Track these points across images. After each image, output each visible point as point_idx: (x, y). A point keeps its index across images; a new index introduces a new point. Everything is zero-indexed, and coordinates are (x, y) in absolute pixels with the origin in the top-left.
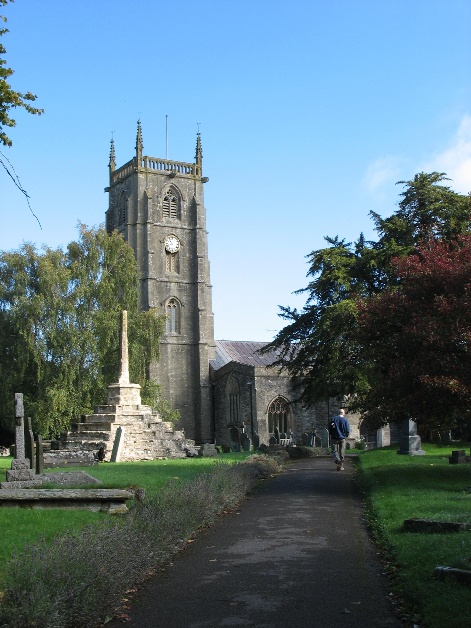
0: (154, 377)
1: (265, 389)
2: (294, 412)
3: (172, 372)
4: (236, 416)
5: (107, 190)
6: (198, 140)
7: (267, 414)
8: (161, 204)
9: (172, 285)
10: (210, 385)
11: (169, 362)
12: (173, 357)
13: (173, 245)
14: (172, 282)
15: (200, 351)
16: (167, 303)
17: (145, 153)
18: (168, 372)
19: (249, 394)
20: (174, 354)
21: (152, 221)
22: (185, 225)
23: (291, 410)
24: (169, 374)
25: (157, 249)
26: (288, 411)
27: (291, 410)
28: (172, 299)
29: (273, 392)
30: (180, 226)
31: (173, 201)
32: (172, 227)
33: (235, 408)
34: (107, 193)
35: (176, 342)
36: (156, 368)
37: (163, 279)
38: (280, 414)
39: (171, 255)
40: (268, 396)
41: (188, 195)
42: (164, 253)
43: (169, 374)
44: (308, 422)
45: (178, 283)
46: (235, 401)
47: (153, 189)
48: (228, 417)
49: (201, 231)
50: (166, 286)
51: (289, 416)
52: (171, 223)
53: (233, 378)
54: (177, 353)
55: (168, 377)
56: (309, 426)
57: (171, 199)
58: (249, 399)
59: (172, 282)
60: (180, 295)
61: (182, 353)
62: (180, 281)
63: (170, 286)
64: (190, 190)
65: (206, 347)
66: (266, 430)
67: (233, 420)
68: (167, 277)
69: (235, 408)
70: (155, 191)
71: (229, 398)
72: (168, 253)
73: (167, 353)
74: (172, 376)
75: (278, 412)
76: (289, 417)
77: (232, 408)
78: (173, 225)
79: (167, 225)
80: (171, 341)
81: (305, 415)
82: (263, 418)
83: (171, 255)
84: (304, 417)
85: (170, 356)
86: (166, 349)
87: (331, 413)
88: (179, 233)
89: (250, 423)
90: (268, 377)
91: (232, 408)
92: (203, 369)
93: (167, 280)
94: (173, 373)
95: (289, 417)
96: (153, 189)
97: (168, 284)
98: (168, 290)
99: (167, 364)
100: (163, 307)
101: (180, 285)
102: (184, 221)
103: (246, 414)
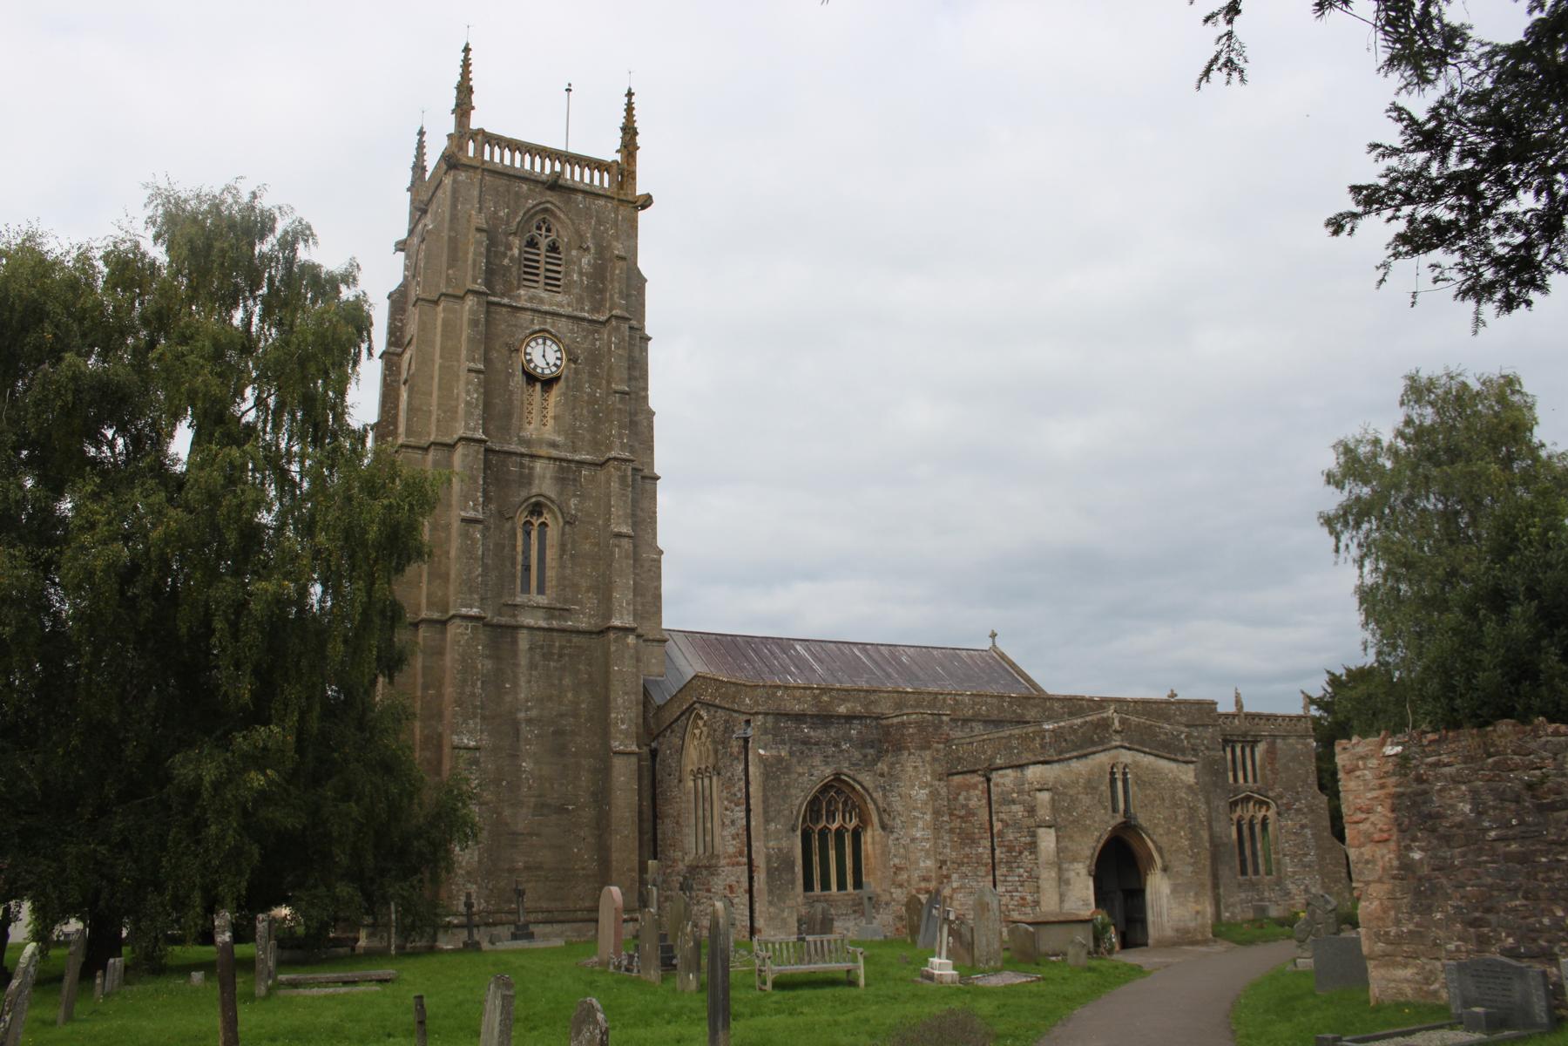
0: (465, 721)
1: (791, 753)
2: (884, 827)
3: (528, 709)
4: (708, 838)
5: (401, 246)
6: (630, 109)
7: (799, 832)
8: (516, 252)
9: (539, 466)
10: (645, 750)
11: (522, 681)
12: (533, 666)
13: (544, 356)
14: (540, 457)
15: (613, 648)
16: (521, 518)
17: (475, 123)
18: (518, 710)
19: (741, 767)
20: (537, 658)
21: (483, 289)
22: (582, 310)
23: (875, 819)
24: (521, 715)
25: (499, 366)
26: (864, 822)
27: (875, 819)
28: (538, 504)
29: (817, 761)
30: (568, 310)
31: (553, 248)
32: (546, 313)
33: (708, 814)
34: (402, 254)
35: (543, 624)
36: (473, 695)
37: (513, 447)
38: (839, 834)
39: (538, 386)
40: (800, 775)
41: (594, 235)
42: (519, 378)
43: (521, 715)
44: (928, 856)
45: (555, 459)
46: (707, 793)
47: (495, 212)
48: (690, 842)
49: (625, 327)
50: (522, 466)
51: (869, 839)
52: (542, 301)
53: (701, 723)
54: (547, 656)
55: (515, 725)
56: (928, 869)
57: (544, 243)
58: (742, 784)
59: (540, 457)
60: (560, 494)
61: (561, 656)
62: (563, 455)
63: (531, 469)
64: (599, 222)
65: (631, 639)
66: (793, 882)
67: (701, 851)
68: (528, 443)
69: (708, 814)
70: (498, 218)
71: (691, 784)
72: (531, 378)
73: (515, 653)
74: (529, 721)
75: (835, 826)
76: (869, 840)
77: (700, 813)
78: (546, 308)
79: (529, 305)
80: (532, 622)
81: (918, 835)
82: (784, 844)
83: (538, 386)
84: (913, 840)
85: (523, 661)
86: (514, 642)
87: (997, 826)
88: (564, 330)
89: (745, 860)
90: (799, 718)
91: (700, 813)
92: (620, 701)
93: (523, 450)
94: (534, 713)
95: (869, 840)
96: (495, 212)
97: (526, 461)
98: (527, 479)
99: (515, 685)
100: (508, 525)
101: (561, 468)
102: (580, 300)
103: (733, 830)
